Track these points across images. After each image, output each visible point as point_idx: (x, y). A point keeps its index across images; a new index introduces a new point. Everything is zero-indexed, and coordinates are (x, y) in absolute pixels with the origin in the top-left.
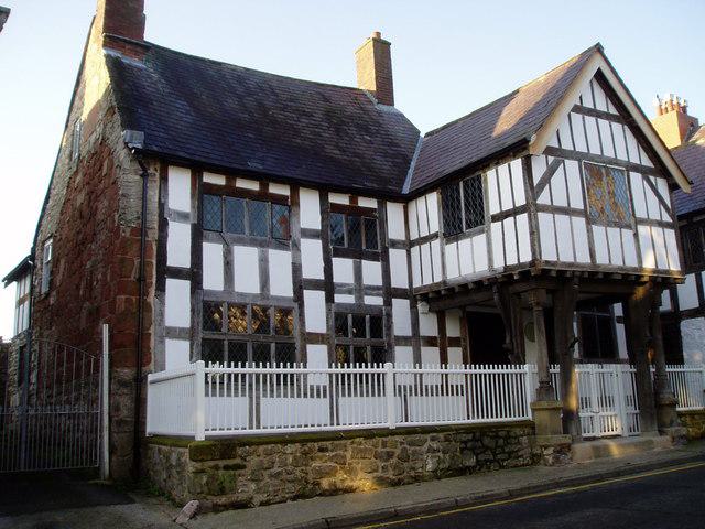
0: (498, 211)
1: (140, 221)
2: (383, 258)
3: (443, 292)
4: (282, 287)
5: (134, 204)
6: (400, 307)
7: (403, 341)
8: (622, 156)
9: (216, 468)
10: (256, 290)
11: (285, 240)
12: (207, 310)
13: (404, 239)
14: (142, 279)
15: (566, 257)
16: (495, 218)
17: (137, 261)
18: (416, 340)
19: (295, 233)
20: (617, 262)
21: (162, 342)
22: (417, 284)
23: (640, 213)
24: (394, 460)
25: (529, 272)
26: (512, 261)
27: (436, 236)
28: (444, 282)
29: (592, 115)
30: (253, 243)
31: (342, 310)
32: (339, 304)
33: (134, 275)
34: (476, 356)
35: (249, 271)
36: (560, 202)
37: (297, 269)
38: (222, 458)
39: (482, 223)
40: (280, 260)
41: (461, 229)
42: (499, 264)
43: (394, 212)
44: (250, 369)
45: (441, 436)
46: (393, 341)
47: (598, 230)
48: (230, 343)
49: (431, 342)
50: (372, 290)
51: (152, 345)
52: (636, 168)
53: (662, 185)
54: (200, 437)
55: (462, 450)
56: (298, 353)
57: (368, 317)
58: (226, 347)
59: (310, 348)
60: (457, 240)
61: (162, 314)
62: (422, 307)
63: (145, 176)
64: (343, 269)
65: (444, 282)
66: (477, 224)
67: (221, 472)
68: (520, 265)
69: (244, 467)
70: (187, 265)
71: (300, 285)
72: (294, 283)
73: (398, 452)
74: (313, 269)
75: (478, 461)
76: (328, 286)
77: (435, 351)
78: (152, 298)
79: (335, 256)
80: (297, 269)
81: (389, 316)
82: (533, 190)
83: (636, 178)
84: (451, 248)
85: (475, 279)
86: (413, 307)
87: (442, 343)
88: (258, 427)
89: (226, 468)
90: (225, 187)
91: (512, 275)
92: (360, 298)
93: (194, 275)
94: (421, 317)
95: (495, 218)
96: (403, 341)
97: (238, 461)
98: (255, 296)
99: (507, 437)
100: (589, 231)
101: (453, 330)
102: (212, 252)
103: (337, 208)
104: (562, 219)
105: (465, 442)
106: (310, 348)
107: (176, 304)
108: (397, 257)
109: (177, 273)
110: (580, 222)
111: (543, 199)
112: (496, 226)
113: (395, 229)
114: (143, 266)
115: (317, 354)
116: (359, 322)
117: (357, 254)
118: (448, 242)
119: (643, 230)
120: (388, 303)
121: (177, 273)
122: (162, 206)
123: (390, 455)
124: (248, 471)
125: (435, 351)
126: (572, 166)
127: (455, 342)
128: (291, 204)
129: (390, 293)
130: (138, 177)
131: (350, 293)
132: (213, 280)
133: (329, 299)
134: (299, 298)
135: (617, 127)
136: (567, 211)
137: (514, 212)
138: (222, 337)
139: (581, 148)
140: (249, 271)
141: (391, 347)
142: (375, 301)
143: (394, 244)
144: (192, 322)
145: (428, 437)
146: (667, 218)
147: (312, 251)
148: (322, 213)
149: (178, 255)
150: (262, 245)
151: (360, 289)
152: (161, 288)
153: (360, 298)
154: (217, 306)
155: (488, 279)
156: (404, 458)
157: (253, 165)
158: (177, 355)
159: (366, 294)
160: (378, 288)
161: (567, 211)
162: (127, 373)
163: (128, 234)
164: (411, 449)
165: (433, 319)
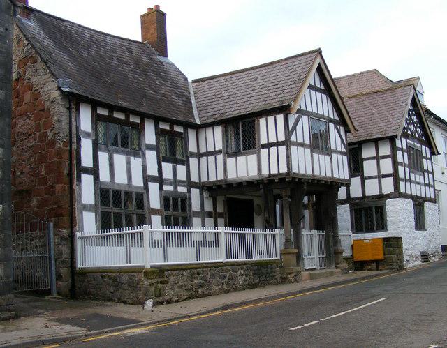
2: (185, 162)
4: (138, 181)
5: (65, 126)
6: (195, 193)
7: (197, 214)
8: (326, 114)
9: (157, 282)
10: (125, 182)
11: (139, 152)
14: (70, 174)
15: (302, 172)
16: (264, 146)
18: (202, 214)
19: (143, 147)
20: (323, 174)
21: (81, 213)
22: (204, 179)
23: (333, 147)
24: (226, 280)
25: (285, 178)
26: (274, 171)
27: (220, 152)
30: (123, 153)
33: (66, 171)
34: (231, 223)
35: (124, 170)
36: (300, 140)
39: (254, 148)
40: (136, 163)
42: (265, 172)
43: (191, 135)
44: (124, 231)
47: (315, 155)
49: (209, 215)
52: (332, 121)
53: (342, 130)
56: (147, 219)
57: (180, 199)
61: (80, 196)
62: (205, 194)
63: (69, 109)
64: (167, 168)
66: (251, 148)
67: (160, 285)
68: (279, 174)
69: (167, 282)
71: (147, 179)
72: (144, 178)
74: (153, 171)
75: (260, 281)
76: (160, 180)
77: (212, 220)
78: (75, 187)
79: (164, 161)
81: (190, 198)
82: (288, 132)
83: (332, 126)
84: (231, 161)
85: (248, 180)
86: (201, 194)
87: (214, 215)
89: (161, 283)
90: (124, 120)
91: (274, 180)
92: (176, 188)
93: (95, 171)
95: (264, 146)
96: (197, 214)
97: (166, 279)
98: (125, 185)
100: (312, 156)
101: (220, 209)
102: (103, 157)
103: (163, 131)
104: (301, 149)
107: (87, 191)
108: (193, 162)
109: (87, 171)
110: (308, 151)
112: (264, 151)
113: (192, 147)
114: (71, 165)
115: (156, 220)
117: (174, 160)
119: (334, 156)
120: (189, 191)
121: (87, 171)
122: (78, 128)
123: (225, 277)
124: (169, 285)
125: (212, 220)
127: (221, 215)
128: (140, 129)
129: (190, 185)
132: (104, 176)
133: (161, 188)
134: (146, 187)
135: (324, 96)
136: (302, 145)
137: (277, 144)
138: (110, 210)
139: (309, 109)
140: (124, 170)
141: (191, 218)
142: (182, 189)
143: (192, 155)
144: (96, 201)
145: (240, 267)
146: (344, 150)
147: (151, 156)
149: (87, 161)
150: (127, 154)
151: (176, 183)
152: (79, 180)
153: (176, 188)
154: (107, 191)
155: (257, 181)
158: (89, 223)
160: (184, 182)
161: (302, 145)
162: (65, 232)
163: (61, 146)
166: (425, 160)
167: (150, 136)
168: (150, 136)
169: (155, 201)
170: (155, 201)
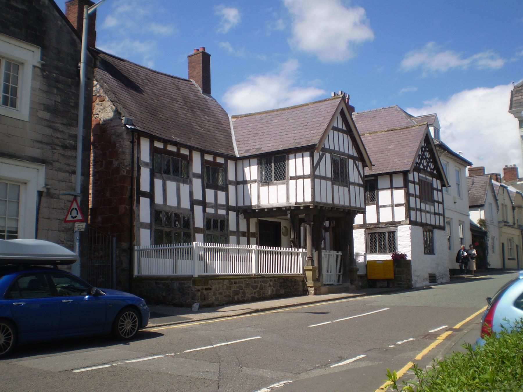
0: (294, 175)
1: (131, 167)
2: (225, 189)
3: (257, 211)
4: (186, 204)
5: (128, 157)
6: (232, 215)
7: (233, 233)
8: (346, 152)
9: (203, 289)
10: (175, 204)
11: (187, 180)
12: (156, 213)
13: (234, 180)
14: (131, 197)
15: (324, 201)
16: (292, 178)
17: (129, 187)
18: (238, 233)
19: (191, 175)
20: (342, 203)
21: (139, 230)
22: (240, 204)
23: (351, 180)
24: (258, 289)
25: (309, 206)
26: (300, 200)
27: (255, 181)
28: (258, 206)
29: (336, 131)
30: (174, 180)
31: (210, 217)
32: (208, 213)
33: (127, 195)
34: (261, 243)
35: (173, 194)
36: (323, 174)
37: (191, 194)
38: (205, 285)
39: (284, 179)
40: (185, 188)
41: (271, 181)
42: (292, 201)
43: (231, 165)
44: (173, 246)
45: (273, 279)
46: (229, 233)
47: (336, 187)
48: (165, 231)
49: (244, 234)
50: (222, 206)
51: (135, 231)
52: (352, 157)
53: (360, 165)
54: (196, 276)
55: (280, 286)
56: (192, 236)
57: (219, 220)
58: (377, 250)
59: (197, 235)
60: (268, 185)
61: (139, 216)
62: (241, 216)
63: (132, 142)
64: (210, 193)
65: (258, 206)
66: (281, 179)
67: (205, 292)
68: (304, 203)
69: (210, 289)
70: (148, 190)
71: (193, 202)
72: (190, 201)
73: (259, 285)
74: (198, 196)
75: (285, 292)
76: (203, 203)
77: (245, 239)
78: (135, 207)
79: (207, 188)
80: (191, 194)
81: (228, 220)
82: (314, 167)
83: (351, 161)
84: (264, 189)
85: (278, 206)
86: (237, 216)
87: (248, 235)
88: (176, 273)
89: (206, 289)
90: (176, 153)
91: (300, 207)
92: (216, 211)
93: (151, 195)
94: (240, 220)
95: (292, 178)
96: (233, 233)
97: (209, 286)
98: (174, 207)
99: (295, 282)
100: (333, 188)
101: (253, 229)
102: (158, 183)
103: (208, 162)
104: (323, 182)
105: (281, 283)
106: (197, 235)
107: (144, 212)
108: (231, 189)
109: (144, 194)
110: (329, 183)
111: (317, 173)
112: (292, 183)
113: (231, 177)
114: (132, 189)
115: (199, 236)
116: (215, 222)
117: (216, 188)
118: (263, 185)
119: (352, 187)
120: (227, 214)
121: (144, 194)
122: (139, 158)
123: (257, 287)
124: (212, 291)
125: (245, 239)
126: (328, 155)
127: (253, 235)
128: (189, 160)
129: (228, 208)
130: (129, 143)
131: (212, 207)
132: (159, 200)
133: (204, 211)
134: (192, 210)
135: (345, 136)
136: (325, 178)
137: (303, 177)
138: (162, 228)
139: (332, 148)
140: (173, 194)
141: (228, 237)
142: (222, 212)
143: (231, 183)
144: (151, 220)
145: (269, 279)
146: (361, 182)
147: (197, 183)
148: (202, 165)
149: (145, 187)
150: (177, 181)
151: (216, 206)
152: (138, 202)
153: (216, 211)
154: (161, 212)
155: (285, 207)
156: (261, 289)
157: (174, 138)
158: (145, 238)
159: (220, 209)
160: (223, 206)
161: (325, 178)
162: (125, 245)
163: (125, 174)
164: (263, 284)
165: (245, 221)
166: (435, 192)
167: (197, 167)
168: (197, 167)
169: (199, 222)
170: (199, 222)
